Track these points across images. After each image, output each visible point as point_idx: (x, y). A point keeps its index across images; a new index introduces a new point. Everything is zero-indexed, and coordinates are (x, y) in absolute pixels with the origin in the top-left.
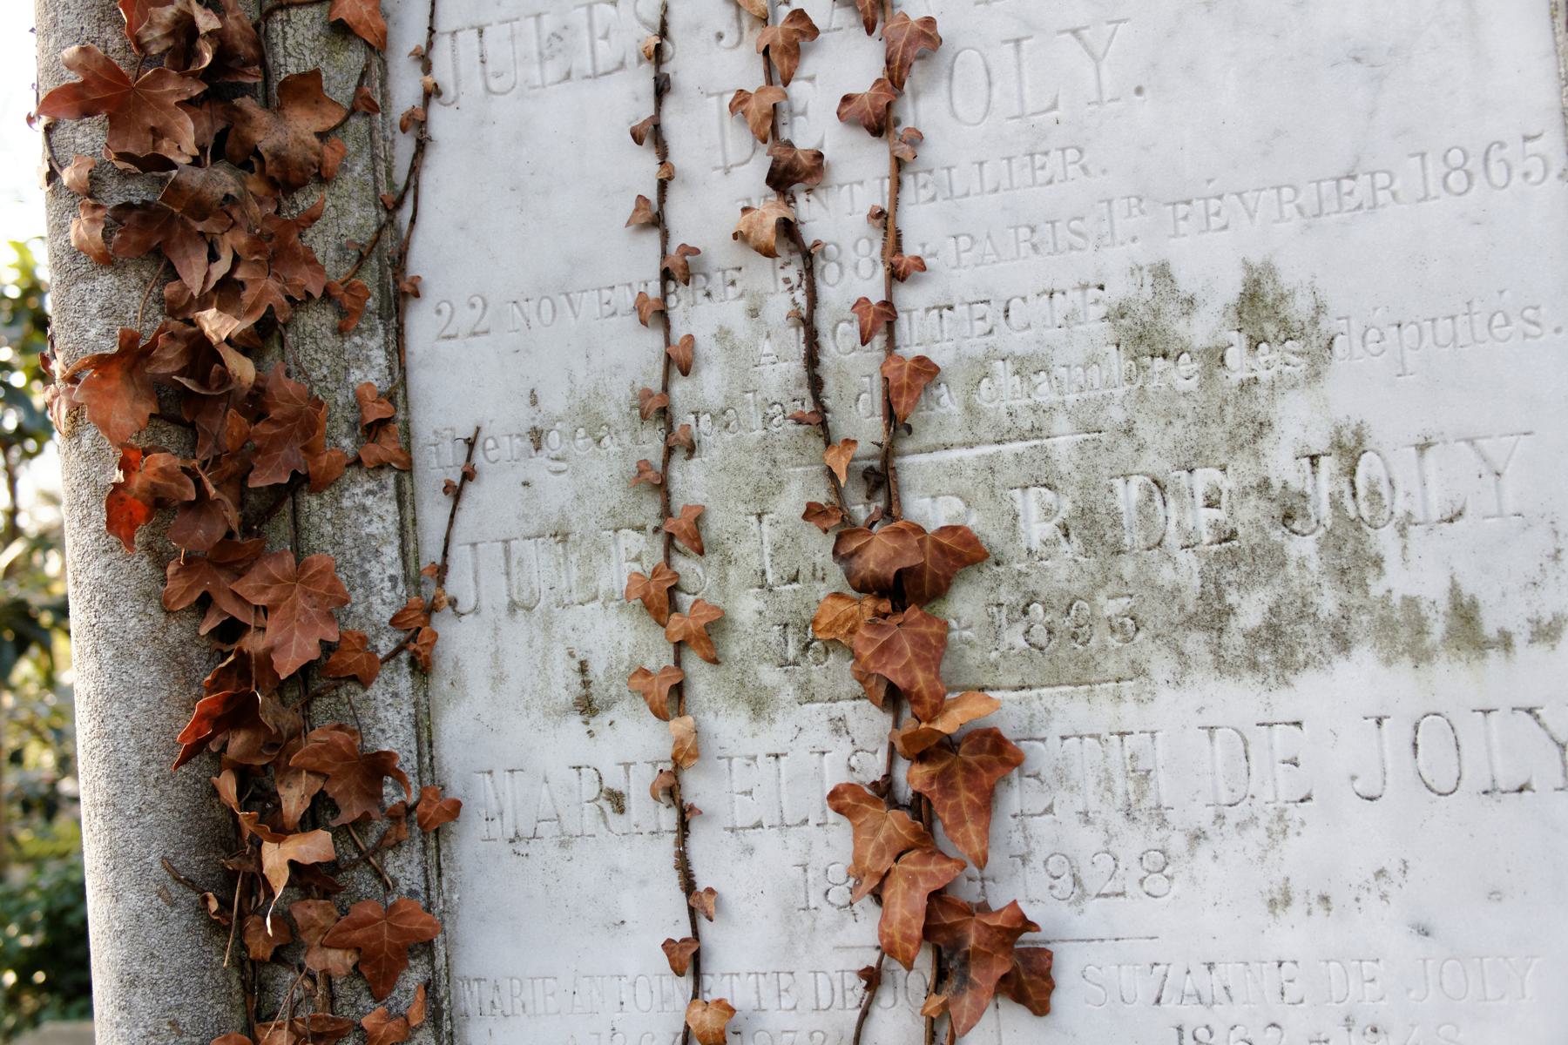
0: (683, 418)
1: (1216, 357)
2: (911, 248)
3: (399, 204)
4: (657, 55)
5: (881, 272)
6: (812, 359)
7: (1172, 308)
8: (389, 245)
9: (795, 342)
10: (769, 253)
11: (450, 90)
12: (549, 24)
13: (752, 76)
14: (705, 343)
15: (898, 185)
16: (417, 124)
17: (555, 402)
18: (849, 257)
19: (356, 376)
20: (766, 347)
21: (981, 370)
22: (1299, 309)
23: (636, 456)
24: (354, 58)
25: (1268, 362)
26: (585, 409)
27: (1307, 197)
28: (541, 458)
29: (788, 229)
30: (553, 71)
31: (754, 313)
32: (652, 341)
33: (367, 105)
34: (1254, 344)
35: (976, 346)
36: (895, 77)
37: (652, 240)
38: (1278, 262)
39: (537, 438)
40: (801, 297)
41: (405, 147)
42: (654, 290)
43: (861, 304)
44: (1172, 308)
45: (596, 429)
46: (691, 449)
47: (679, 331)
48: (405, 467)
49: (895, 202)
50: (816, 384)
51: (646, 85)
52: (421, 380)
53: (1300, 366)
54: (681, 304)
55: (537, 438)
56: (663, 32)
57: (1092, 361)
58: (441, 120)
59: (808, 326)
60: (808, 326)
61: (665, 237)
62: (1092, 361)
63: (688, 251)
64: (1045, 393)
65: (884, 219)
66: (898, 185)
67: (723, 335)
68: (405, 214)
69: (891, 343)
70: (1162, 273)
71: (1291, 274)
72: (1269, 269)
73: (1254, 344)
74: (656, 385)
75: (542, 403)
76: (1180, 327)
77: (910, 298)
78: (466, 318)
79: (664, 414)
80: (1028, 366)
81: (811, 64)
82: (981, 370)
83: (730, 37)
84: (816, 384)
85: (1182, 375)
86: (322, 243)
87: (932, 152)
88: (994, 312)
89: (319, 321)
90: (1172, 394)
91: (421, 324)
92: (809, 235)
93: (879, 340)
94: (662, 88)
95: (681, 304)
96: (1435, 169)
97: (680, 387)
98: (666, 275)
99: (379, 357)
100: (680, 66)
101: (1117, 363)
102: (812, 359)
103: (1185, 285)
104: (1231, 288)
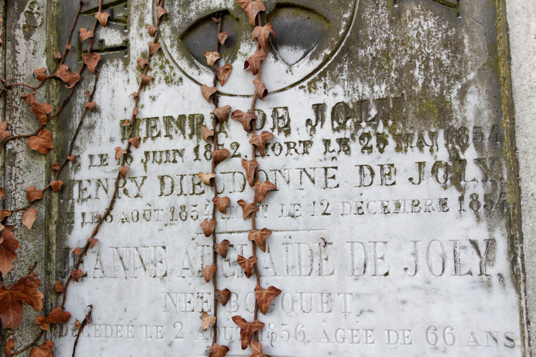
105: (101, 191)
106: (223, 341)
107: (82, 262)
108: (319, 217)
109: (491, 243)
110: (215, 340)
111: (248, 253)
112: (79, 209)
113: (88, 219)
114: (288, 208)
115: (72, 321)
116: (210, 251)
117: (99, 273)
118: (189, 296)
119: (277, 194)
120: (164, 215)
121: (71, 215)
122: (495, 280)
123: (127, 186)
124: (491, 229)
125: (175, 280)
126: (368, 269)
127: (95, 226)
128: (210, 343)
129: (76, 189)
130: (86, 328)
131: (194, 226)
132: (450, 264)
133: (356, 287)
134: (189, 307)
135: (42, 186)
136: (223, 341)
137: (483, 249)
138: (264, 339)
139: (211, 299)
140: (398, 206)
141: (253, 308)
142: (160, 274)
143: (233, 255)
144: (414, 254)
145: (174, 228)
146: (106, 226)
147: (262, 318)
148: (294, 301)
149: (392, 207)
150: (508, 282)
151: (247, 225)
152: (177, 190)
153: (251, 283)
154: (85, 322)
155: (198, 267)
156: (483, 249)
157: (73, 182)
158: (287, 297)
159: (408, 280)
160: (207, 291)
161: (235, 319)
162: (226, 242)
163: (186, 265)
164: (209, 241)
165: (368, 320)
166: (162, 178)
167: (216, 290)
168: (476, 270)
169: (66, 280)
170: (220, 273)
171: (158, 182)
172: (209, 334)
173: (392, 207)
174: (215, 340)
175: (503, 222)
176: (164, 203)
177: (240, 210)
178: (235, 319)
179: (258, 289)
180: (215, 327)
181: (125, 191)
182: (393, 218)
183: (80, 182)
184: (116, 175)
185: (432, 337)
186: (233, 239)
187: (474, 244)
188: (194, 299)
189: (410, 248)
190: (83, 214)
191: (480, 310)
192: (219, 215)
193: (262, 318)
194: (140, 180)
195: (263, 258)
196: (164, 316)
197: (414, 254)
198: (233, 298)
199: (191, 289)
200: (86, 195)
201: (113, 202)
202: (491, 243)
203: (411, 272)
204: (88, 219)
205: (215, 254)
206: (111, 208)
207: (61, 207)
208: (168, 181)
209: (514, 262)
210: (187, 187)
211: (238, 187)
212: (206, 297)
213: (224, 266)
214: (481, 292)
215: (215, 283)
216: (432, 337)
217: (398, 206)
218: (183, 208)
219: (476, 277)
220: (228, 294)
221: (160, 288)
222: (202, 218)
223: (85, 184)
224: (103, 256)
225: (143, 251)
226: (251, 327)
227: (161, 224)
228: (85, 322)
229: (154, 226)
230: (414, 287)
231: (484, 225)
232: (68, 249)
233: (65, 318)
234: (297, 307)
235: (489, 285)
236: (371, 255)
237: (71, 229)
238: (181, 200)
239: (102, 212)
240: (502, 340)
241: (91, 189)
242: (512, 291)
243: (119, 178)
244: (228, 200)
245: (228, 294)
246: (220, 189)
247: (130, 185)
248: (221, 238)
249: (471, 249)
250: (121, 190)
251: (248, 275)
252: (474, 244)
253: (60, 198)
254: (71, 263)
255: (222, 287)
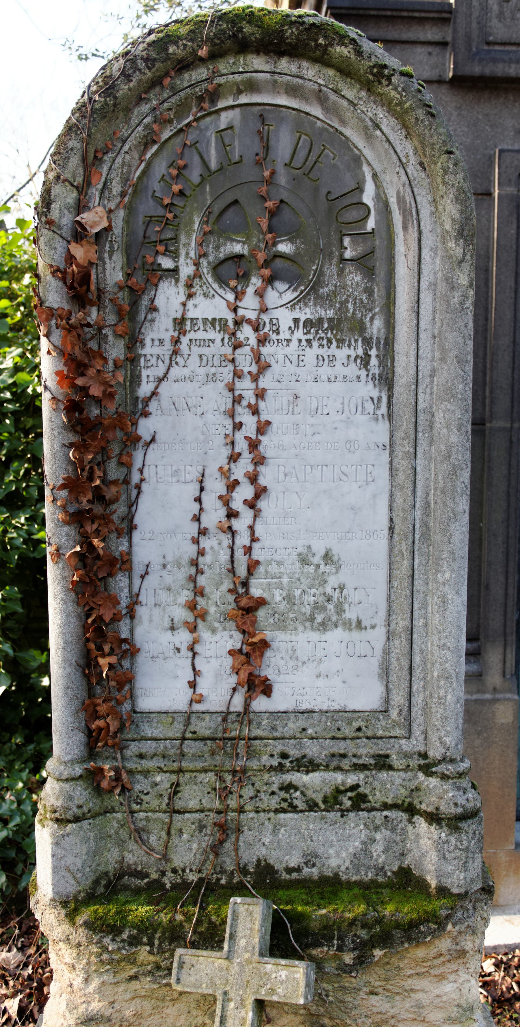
0: (201, 566)
1: (318, 566)
2: (257, 535)
3: (132, 505)
4: (201, 482)
5: (249, 539)
6: (232, 556)
7: (310, 555)
8: (130, 517)
9: (229, 551)
10: (225, 532)
11: (147, 480)
12: (174, 468)
13: (224, 492)
14: (207, 550)
15: (255, 520)
16: (138, 487)
17: (170, 558)
18: (243, 534)
19: (120, 548)
20: (222, 552)
21: (269, 563)
22: (335, 558)
23: (189, 573)
24: (124, 470)
25: (328, 569)
26: (177, 561)
27: (340, 535)
28: (165, 571)
29: (230, 528)
30: (174, 479)
31: (219, 544)
32: (195, 547)
33: (127, 482)
34: (326, 564)
35: (269, 558)
36: (257, 496)
37: (196, 524)
38: (333, 548)
39: (164, 566)
40: (231, 542)
41: (134, 492)
42: (196, 535)
43: (244, 546)
44: (310, 555)
45: (179, 566)
46: (202, 573)
47: (202, 546)
48: (130, 570)
49: (254, 524)
50: (232, 562)
51: (198, 486)
52: (135, 549)
53: (334, 570)
54: (202, 539)
55: (164, 566)
56: (203, 475)
57: (293, 564)
58: (144, 486)
59: (232, 548)
60: (232, 548)
61: (200, 524)
62: (293, 564)
63: (206, 529)
64: (282, 570)
65: (251, 528)
66: (255, 520)
67: (212, 548)
68: (134, 508)
69: (250, 555)
70: (309, 547)
71: (335, 551)
72: (330, 550)
73: (326, 564)
74: (195, 558)
75: (167, 558)
76: (312, 559)
77: (256, 545)
78: (148, 536)
79: (197, 565)
80: (279, 563)
81: (238, 489)
82: (269, 563)
83: (219, 479)
84: (232, 562)
85: (311, 569)
86: (115, 517)
87: (263, 514)
88: (273, 551)
89: (113, 536)
90: (309, 573)
91: (136, 536)
92: (235, 528)
93: (247, 556)
94: (202, 489)
95: (202, 539)
96: (364, 534)
97: (201, 559)
98: (199, 533)
99: (126, 544)
100: (207, 484)
101: (298, 565)
102: (232, 556)
103: (314, 550)
104: (323, 552)
105: (160, 362)
106: (237, 450)
107: (147, 406)
108: (294, 383)
109: (380, 398)
110: (233, 450)
111: (253, 401)
112: (144, 373)
113: (151, 379)
114: (276, 377)
115: (142, 441)
116: (230, 400)
117: (159, 412)
118: (217, 426)
119: (271, 369)
120: (201, 378)
121: (139, 376)
122: (380, 417)
123: (177, 360)
124: (380, 392)
125: (209, 417)
126: (319, 411)
127: (156, 383)
128: (230, 452)
129: (142, 360)
130: (152, 446)
131: (221, 385)
132: (360, 409)
133: (311, 420)
134: (217, 432)
135: (122, 358)
136: (237, 450)
137: (376, 401)
138: (261, 448)
139: (230, 427)
140: (336, 378)
141: (255, 432)
142: (199, 413)
143: (244, 403)
144: (343, 404)
145: (209, 386)
146: (163, 384)
147: (260, 437)
148: (278, 428)
149: (332, 379)
150: (386, 418)
151: (253, 386)
152: (210, 363)
153: (255, 419)
154: (151, 442)
155: (223, 409)
156: (376, 401)
157: (140, 355)
158: (274, 426)
159: (339, 417)
160: (228, 423)
161: (245, 437)
162: (240, 395)
163: (216, 408)
164: (230, 394)
165: (317, 438)
166: (201, 356)
167: (234, 423)
168: (372, 412)
169: (137, 417)
170: (236, 413)
171: (198, 359)
172: (229, 447)
173: (332, 379)
174: (233, 450)
175: (386, 388)
176: (202, 371)
177: (249, 377)
178: (245, 437)
179: (259, 421)
180: (233, 443)
181: (177, 363)
182: (333, 385)
183: (145, 356)
184: (170, 353)
185: (348, 446)
186: (244, 393)
187: (372, 399)
188: (220, 428)
189: (340, 400)
190: (148, 376)
191: (372, 432)
192: (236, 379)
193: (260, 437)
194: (186, 357)
195: (262, 405)
196: (202, 437)
197: (343, 404)
198: (244, 427)
199: (219, 422)
200: (149, 364)
201: (169, 369)
202: (380, 398)
203: (340, 413)
204: (151, 379)
205: (234, 401)
206: (167, 373)
207: (132, 371)
208: (204, 358)
209: (389, 408)
210: (217, 362)
211: (248, 364)
212: (227, 426)
213: (238, 409)
214: (373, 423)
215: (233, 419)
216: (348, 446)
217: (336, 378)
218: (214, 374)
219: (371, 415)
220: (241, 424)
221: (199, 421)
222: (226, 381)
223: (149, 357)
224: (162, 402)
225: (189, 400)
226: (255, 441)
227: (200, 384)
228: (151, 442)
229: (195, 384)
230: (341, 421)
231: (377, 389)
232: (138, 398)
233: (139, 438)
234: (280, 431)
235: (377, 419)
236: (320, 404)
237: (139, 385)
238: (213, 370)
239: (161, 375)
240: (381, 446)
241: (153, 361)
242: (387, 422)
243: (172, 355)
244: (242, 370)
245: (241, 424)
246: (237, 364)
247: (179, 359)
248: (237, 393)
249: (370, 402)
250: (174, 362)
251: (253, 414)
252: (372, 399)
253: (132, 365)
254: (140, 406)
255: (237, 420)
